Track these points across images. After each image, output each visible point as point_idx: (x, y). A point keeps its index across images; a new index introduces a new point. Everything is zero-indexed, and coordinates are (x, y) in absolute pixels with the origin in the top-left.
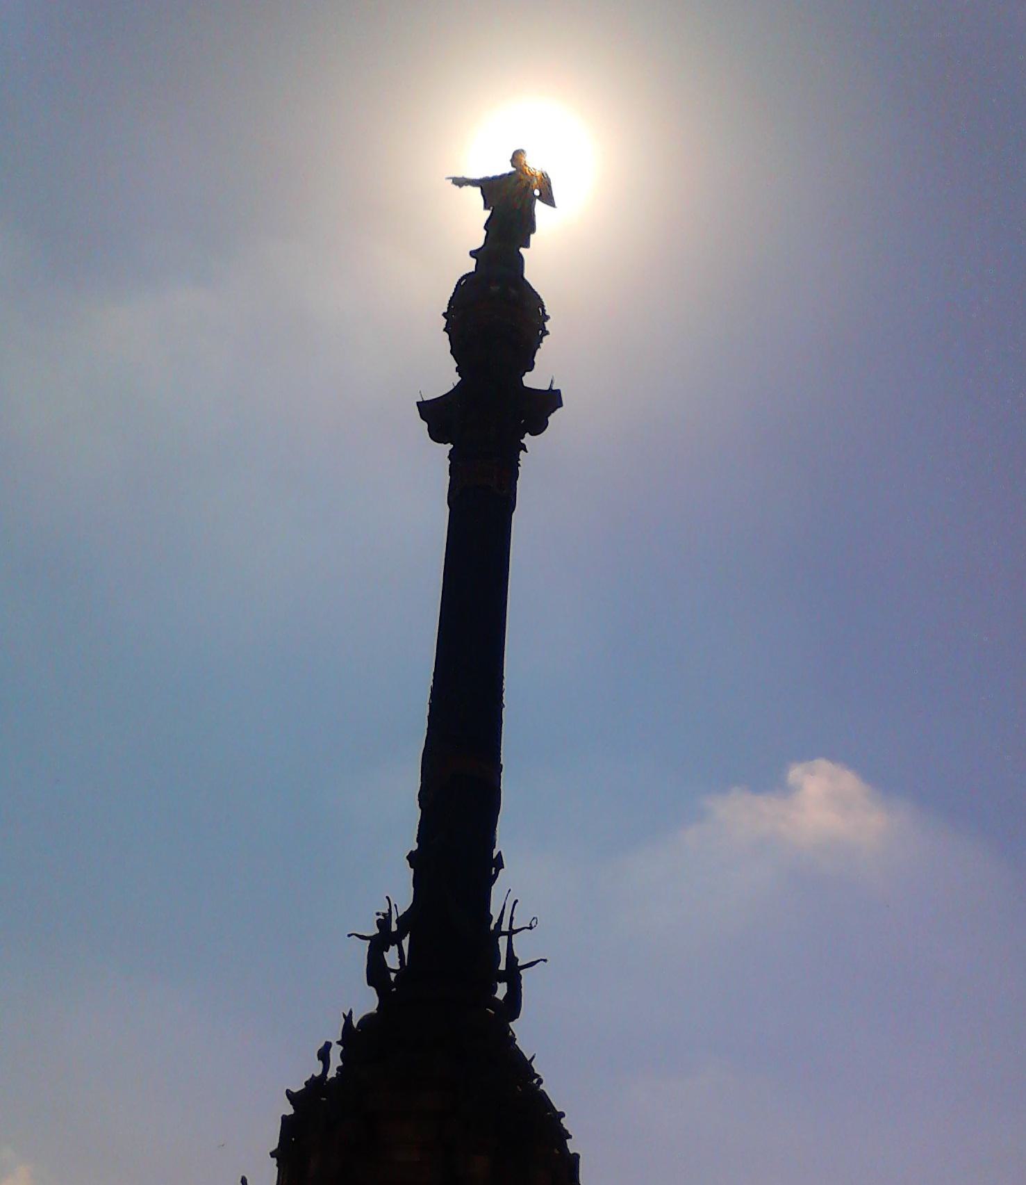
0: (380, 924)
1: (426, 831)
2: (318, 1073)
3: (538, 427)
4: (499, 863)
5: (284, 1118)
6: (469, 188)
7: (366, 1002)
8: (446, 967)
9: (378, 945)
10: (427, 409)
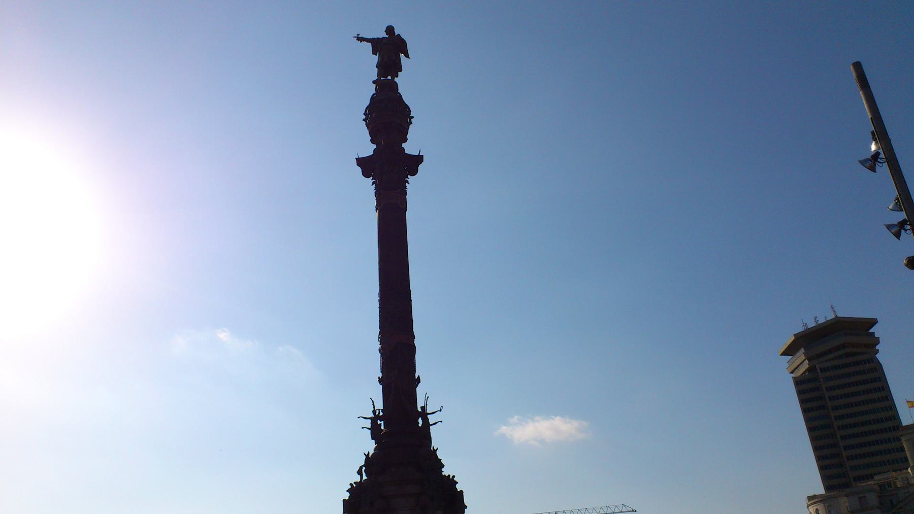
0: (374, 412)
1: (385, 367)
2: (359, 480)
3: (414, 172)
4: (418, 380)
5: (344, 501)
6: (364, 43)
8: (401, 430)
9: (374, 420)
10: (361, 162)
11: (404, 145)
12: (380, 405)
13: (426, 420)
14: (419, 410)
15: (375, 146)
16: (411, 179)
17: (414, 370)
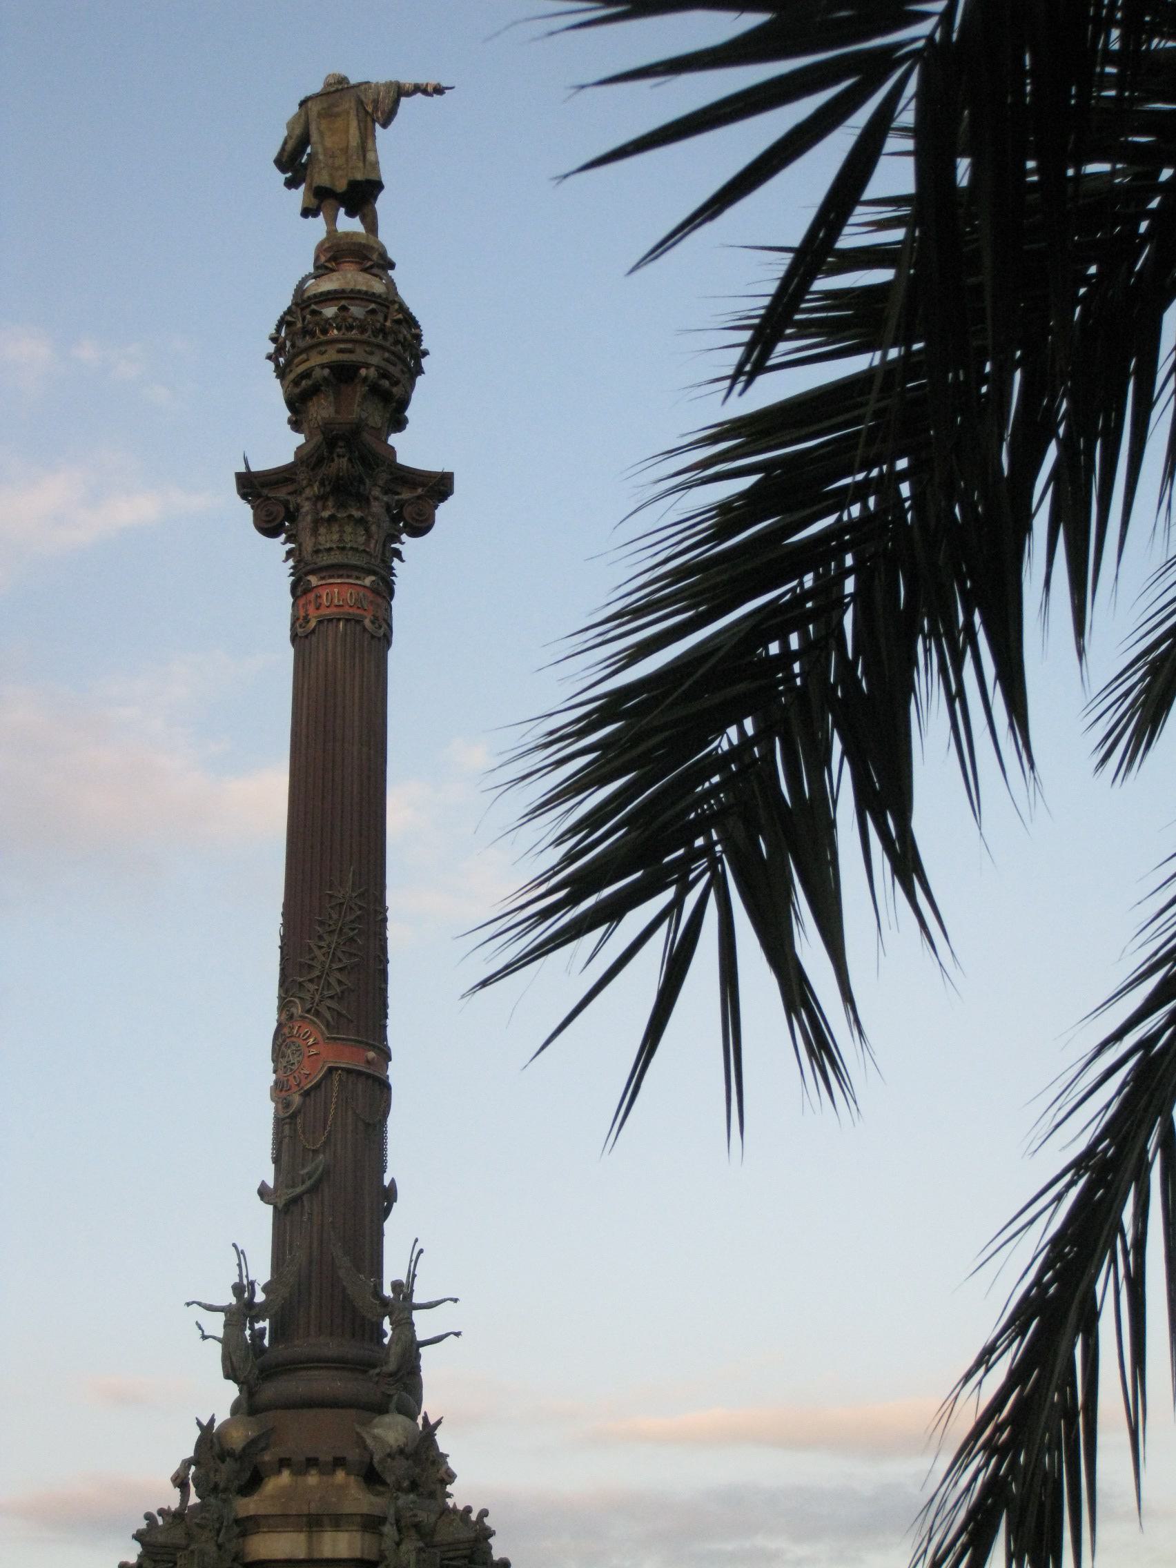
0: (238, 1289)
3: (421, 527)
7: (220, 1398)
8: (325, 1344)
10: (252, 486)
11: (394, 440)
12: (261, 1271)
13: (405, 1325)
14: (388, 1292)
15: (300, 439)
16: (409, 545)
17: (381, 1167)
